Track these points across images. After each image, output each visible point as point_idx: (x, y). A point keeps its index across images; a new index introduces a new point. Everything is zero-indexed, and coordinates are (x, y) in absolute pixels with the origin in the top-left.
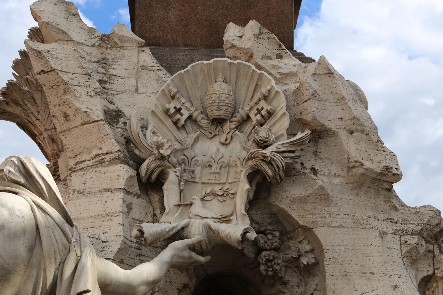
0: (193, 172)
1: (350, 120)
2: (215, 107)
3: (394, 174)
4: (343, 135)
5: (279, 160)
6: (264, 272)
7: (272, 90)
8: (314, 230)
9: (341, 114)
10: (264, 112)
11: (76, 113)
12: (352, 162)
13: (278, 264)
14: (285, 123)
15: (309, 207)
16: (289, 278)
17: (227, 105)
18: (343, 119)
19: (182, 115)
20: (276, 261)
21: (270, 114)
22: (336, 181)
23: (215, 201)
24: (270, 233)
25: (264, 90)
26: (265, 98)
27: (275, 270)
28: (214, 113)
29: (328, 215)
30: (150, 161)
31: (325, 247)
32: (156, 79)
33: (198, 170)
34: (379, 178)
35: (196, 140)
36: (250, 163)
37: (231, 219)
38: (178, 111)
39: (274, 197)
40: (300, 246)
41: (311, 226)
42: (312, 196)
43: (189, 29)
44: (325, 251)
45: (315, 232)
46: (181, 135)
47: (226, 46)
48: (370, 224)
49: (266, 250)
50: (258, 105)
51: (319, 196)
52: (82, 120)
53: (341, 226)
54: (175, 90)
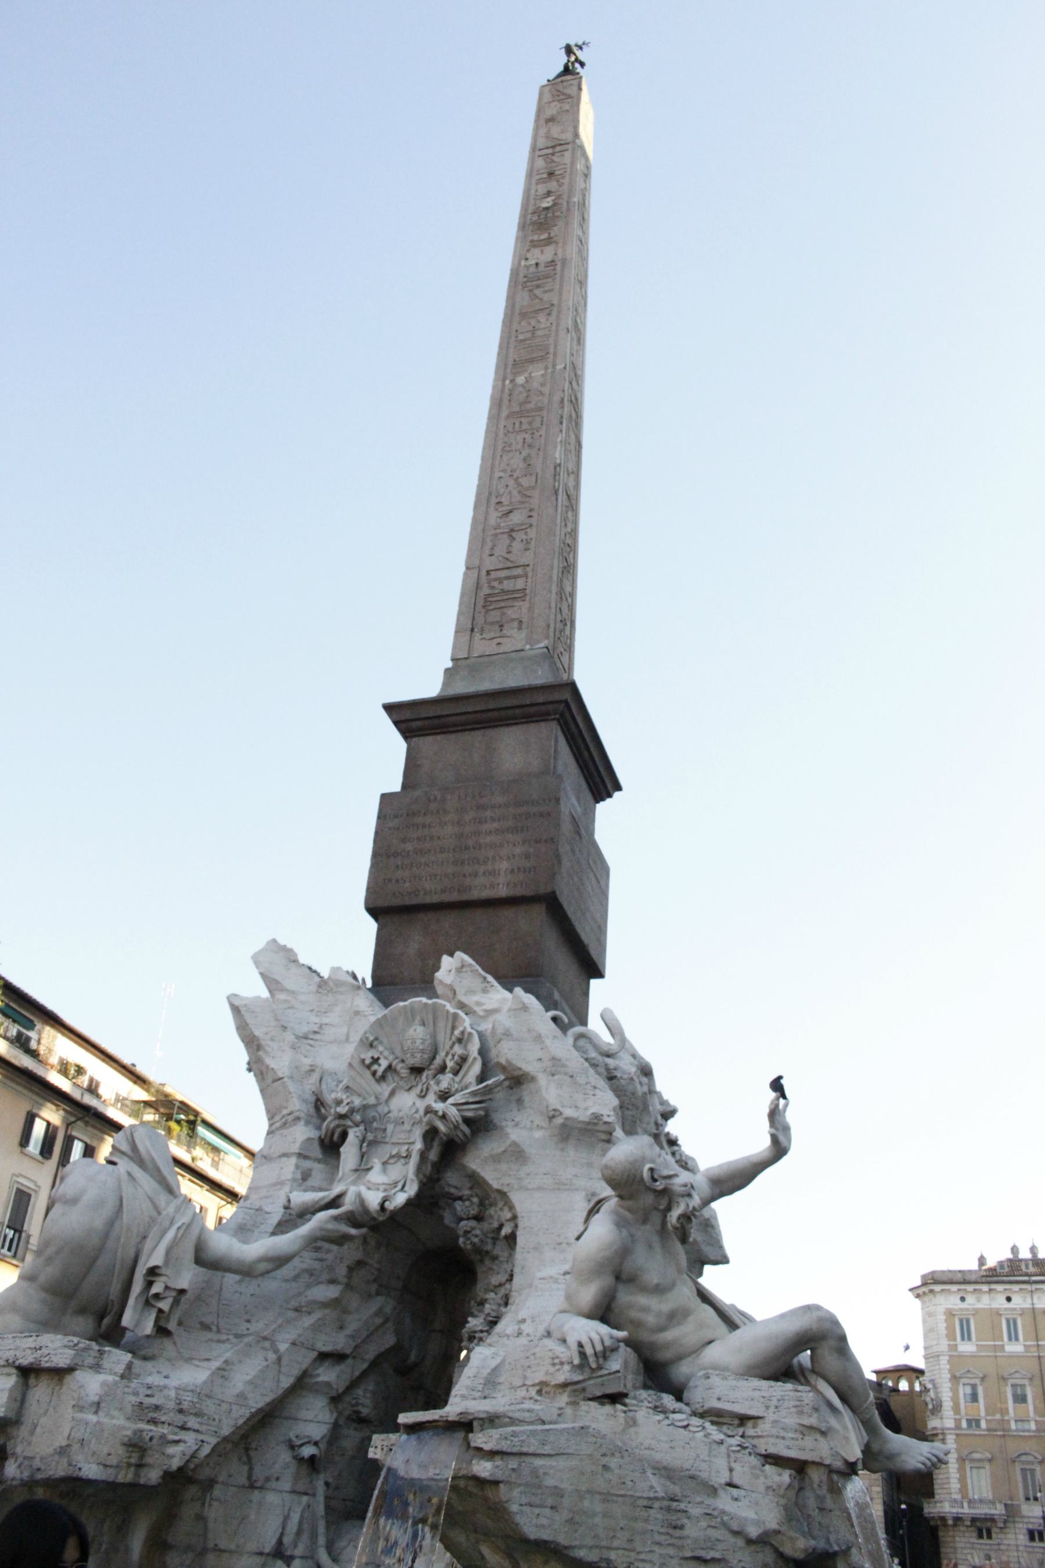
0: (385, 1130)
3: (606, 1123)
6: (462, 1245)
9: (539, 1054)
10: (456, 1058)
13: (476, 1236)
14: (476, 1069)
15: (504, 1166)
17: (422, 1051)
19: (380, 1065)
20: (474, 1232)
22: (538, 1134)
24: (468, 1199)
26: (460, 1040)
28: (411, 1061)
33: (390, 1127)
34: (589, 1127)
35: (392, 1093)
38: (375, 1061)
40: (501, 1213)
41: (505, 1189)
46: (378, 1088)
47: (436, 982)
53: (540, 1189)
54: (371, 1038)
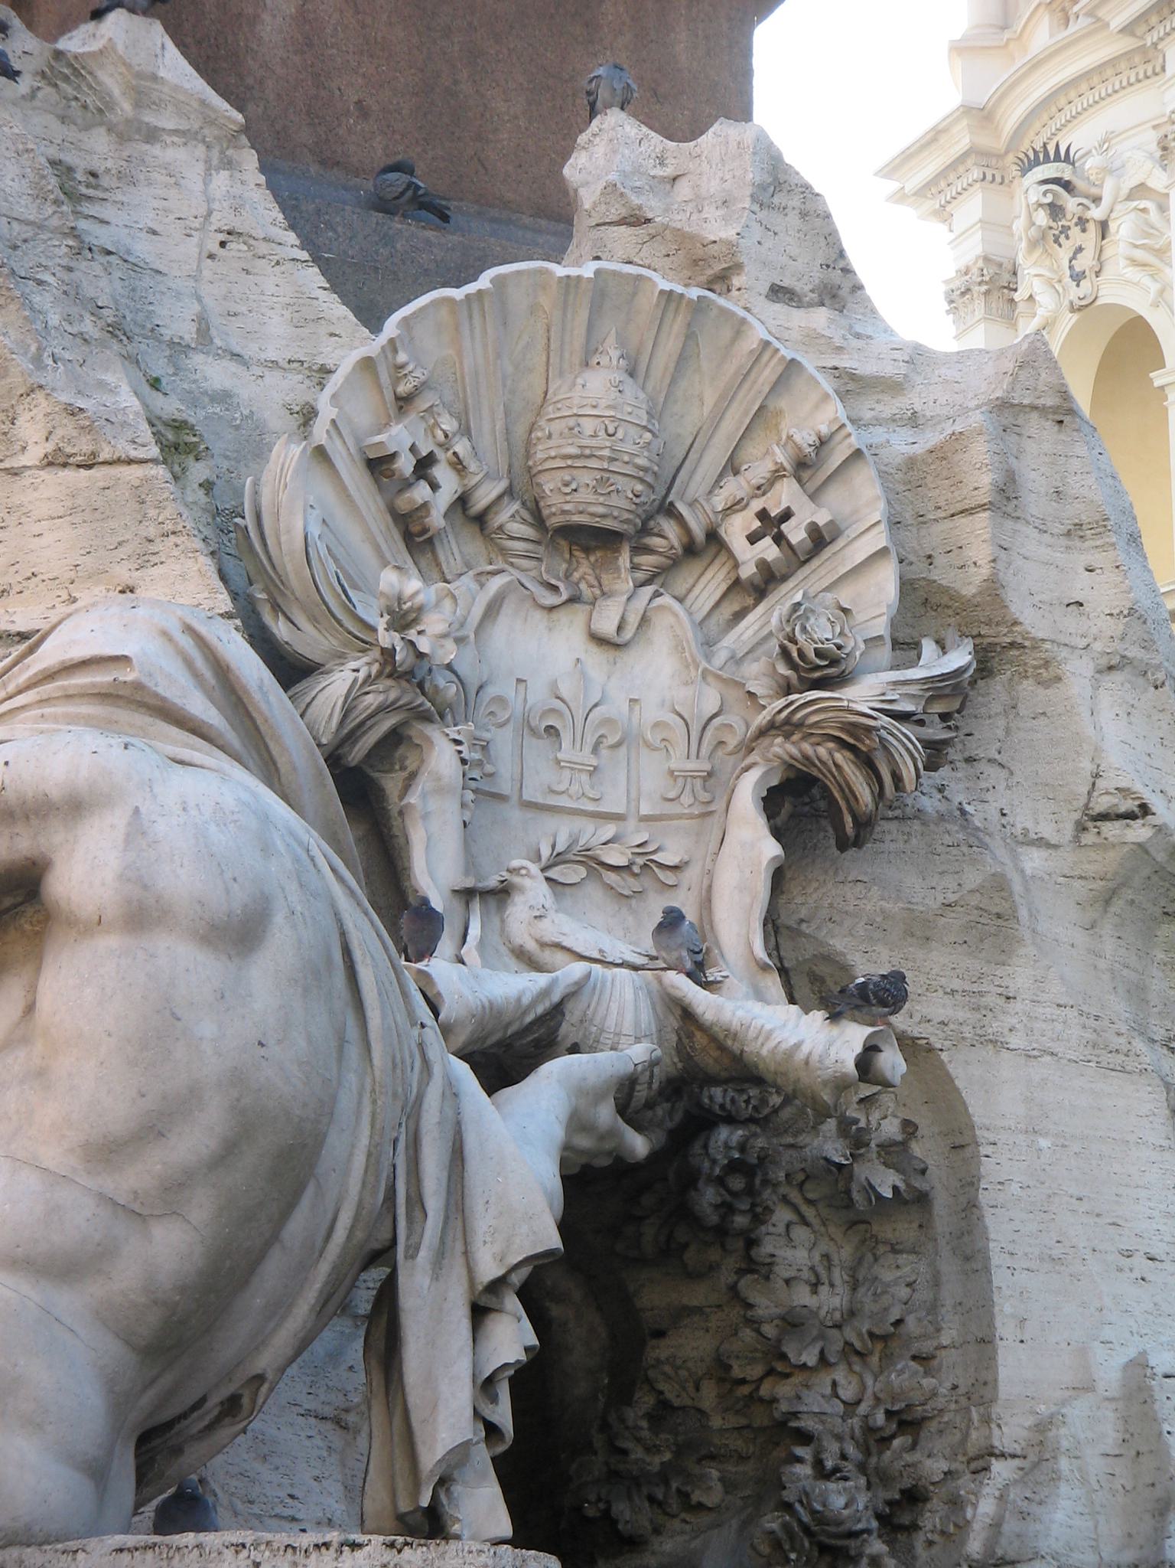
1: (1111, 615)
2: (587, 478)
4: (1078, 671)
5: (907, 750)
7: (833, 443)
8: (944, 1056)
10: (796, 533)
11: (19, 409)
12: (1107, 793)
16: (775, 1247)
18: (1087, 608)
19: (434, 486)
21: (820, 540)
23: (594, 892)
25: (805, 438)
27: (759, 1210)
29: (1001, 1001)
30: (355, 680)
31: (986, 1134)
32: (287, 300)
36: (780, 747)
37: (719, 979)
39: (799, 900)
42: (953, 915)
43: (340, 90)
44: (984, 1150)
45: (951, 1068)
48: (1139, 1053)
49: (731, 1120)
50: (769, 495)
51: (982, 920)
52: (50, 447)
